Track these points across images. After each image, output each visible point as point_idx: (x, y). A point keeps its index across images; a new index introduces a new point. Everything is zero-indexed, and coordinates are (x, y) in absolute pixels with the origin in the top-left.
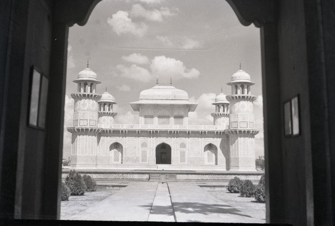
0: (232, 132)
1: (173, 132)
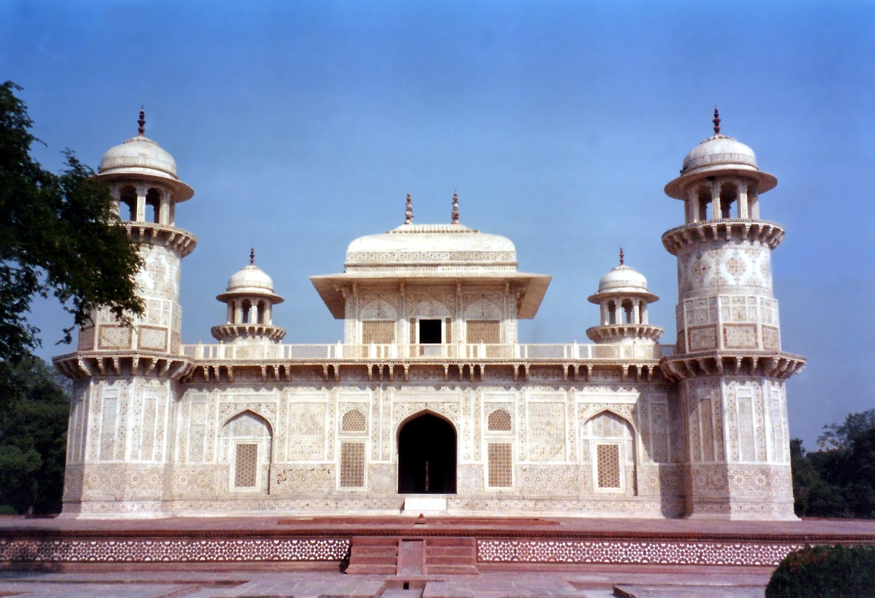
1: (461, 371)
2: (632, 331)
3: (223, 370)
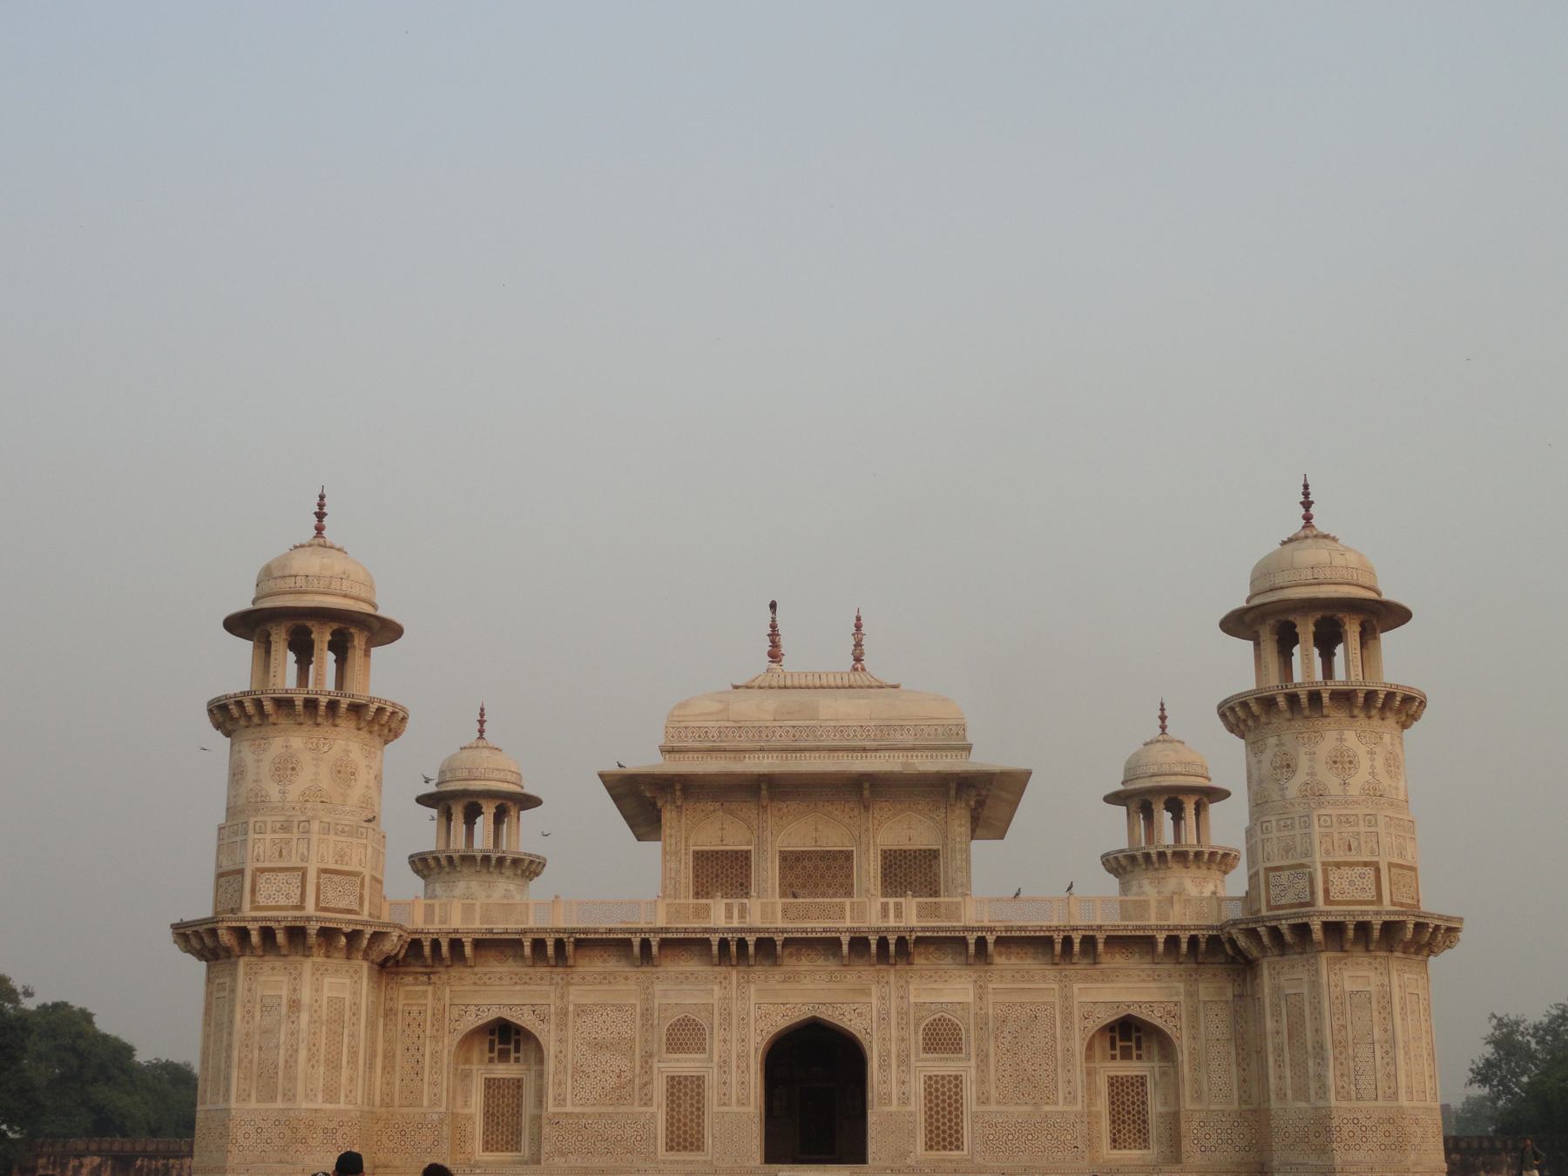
0: (1275, 932)
1: (874, 947)
2: (1181, 856)
3: (456, 945)
